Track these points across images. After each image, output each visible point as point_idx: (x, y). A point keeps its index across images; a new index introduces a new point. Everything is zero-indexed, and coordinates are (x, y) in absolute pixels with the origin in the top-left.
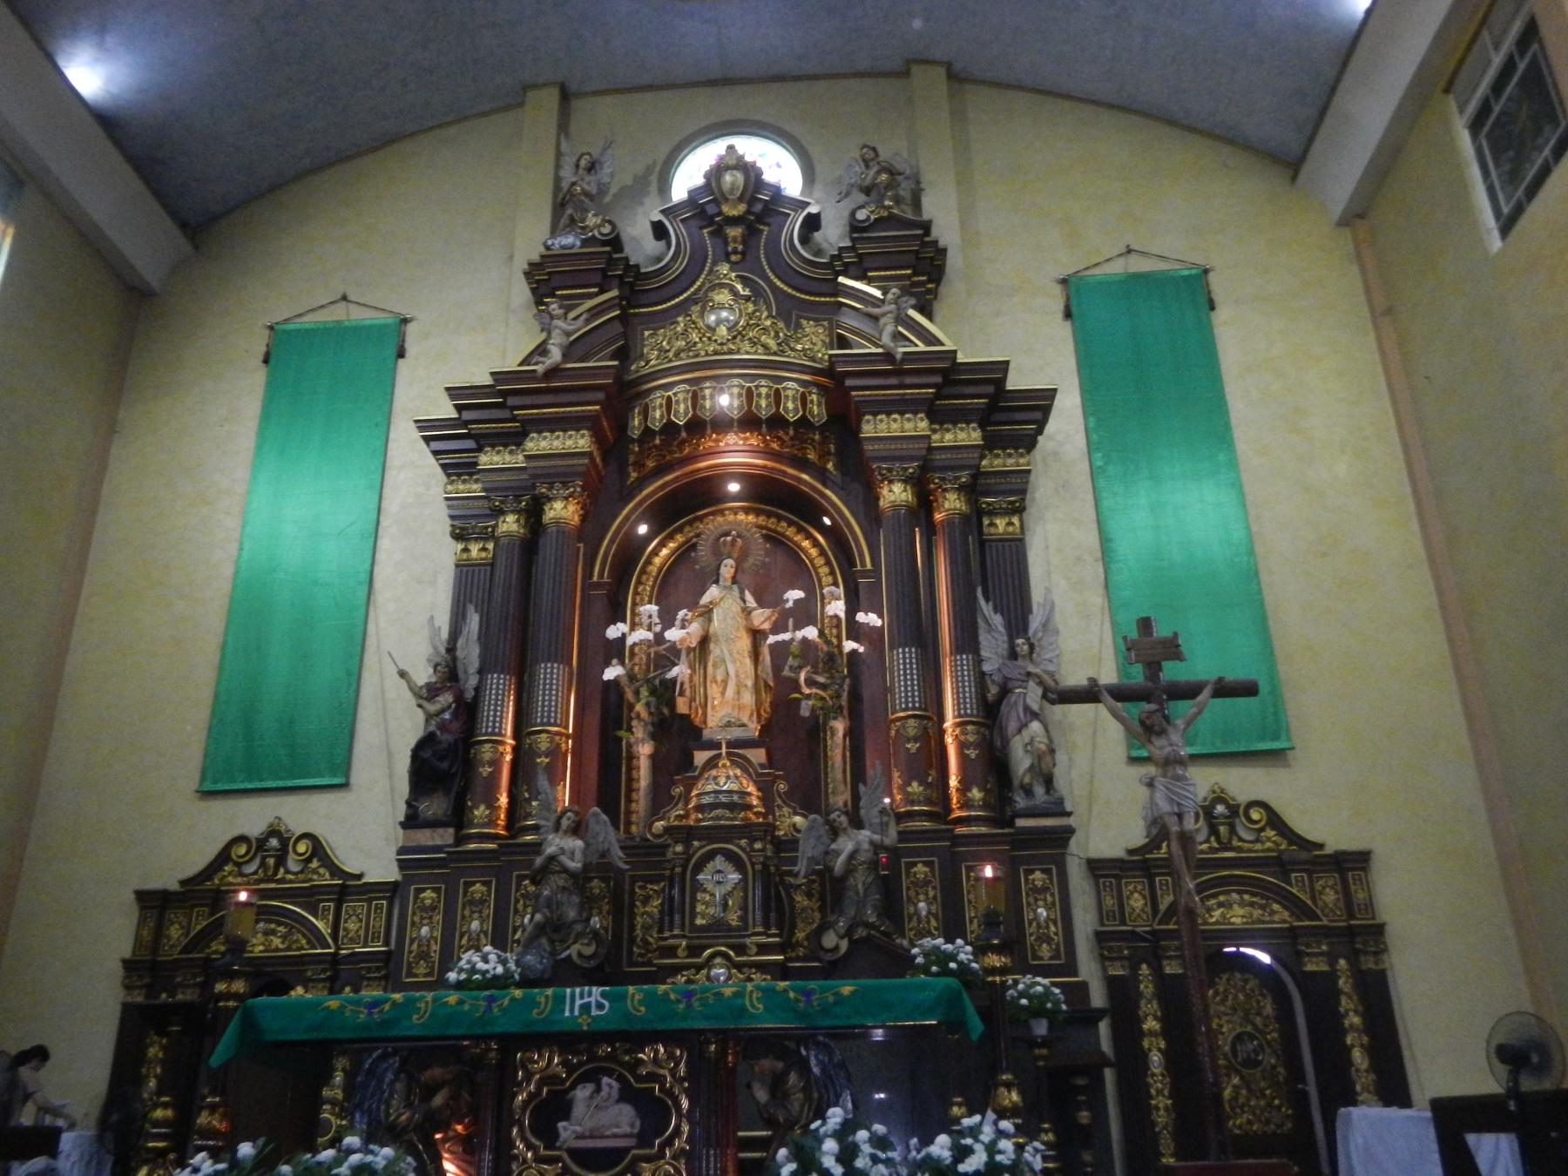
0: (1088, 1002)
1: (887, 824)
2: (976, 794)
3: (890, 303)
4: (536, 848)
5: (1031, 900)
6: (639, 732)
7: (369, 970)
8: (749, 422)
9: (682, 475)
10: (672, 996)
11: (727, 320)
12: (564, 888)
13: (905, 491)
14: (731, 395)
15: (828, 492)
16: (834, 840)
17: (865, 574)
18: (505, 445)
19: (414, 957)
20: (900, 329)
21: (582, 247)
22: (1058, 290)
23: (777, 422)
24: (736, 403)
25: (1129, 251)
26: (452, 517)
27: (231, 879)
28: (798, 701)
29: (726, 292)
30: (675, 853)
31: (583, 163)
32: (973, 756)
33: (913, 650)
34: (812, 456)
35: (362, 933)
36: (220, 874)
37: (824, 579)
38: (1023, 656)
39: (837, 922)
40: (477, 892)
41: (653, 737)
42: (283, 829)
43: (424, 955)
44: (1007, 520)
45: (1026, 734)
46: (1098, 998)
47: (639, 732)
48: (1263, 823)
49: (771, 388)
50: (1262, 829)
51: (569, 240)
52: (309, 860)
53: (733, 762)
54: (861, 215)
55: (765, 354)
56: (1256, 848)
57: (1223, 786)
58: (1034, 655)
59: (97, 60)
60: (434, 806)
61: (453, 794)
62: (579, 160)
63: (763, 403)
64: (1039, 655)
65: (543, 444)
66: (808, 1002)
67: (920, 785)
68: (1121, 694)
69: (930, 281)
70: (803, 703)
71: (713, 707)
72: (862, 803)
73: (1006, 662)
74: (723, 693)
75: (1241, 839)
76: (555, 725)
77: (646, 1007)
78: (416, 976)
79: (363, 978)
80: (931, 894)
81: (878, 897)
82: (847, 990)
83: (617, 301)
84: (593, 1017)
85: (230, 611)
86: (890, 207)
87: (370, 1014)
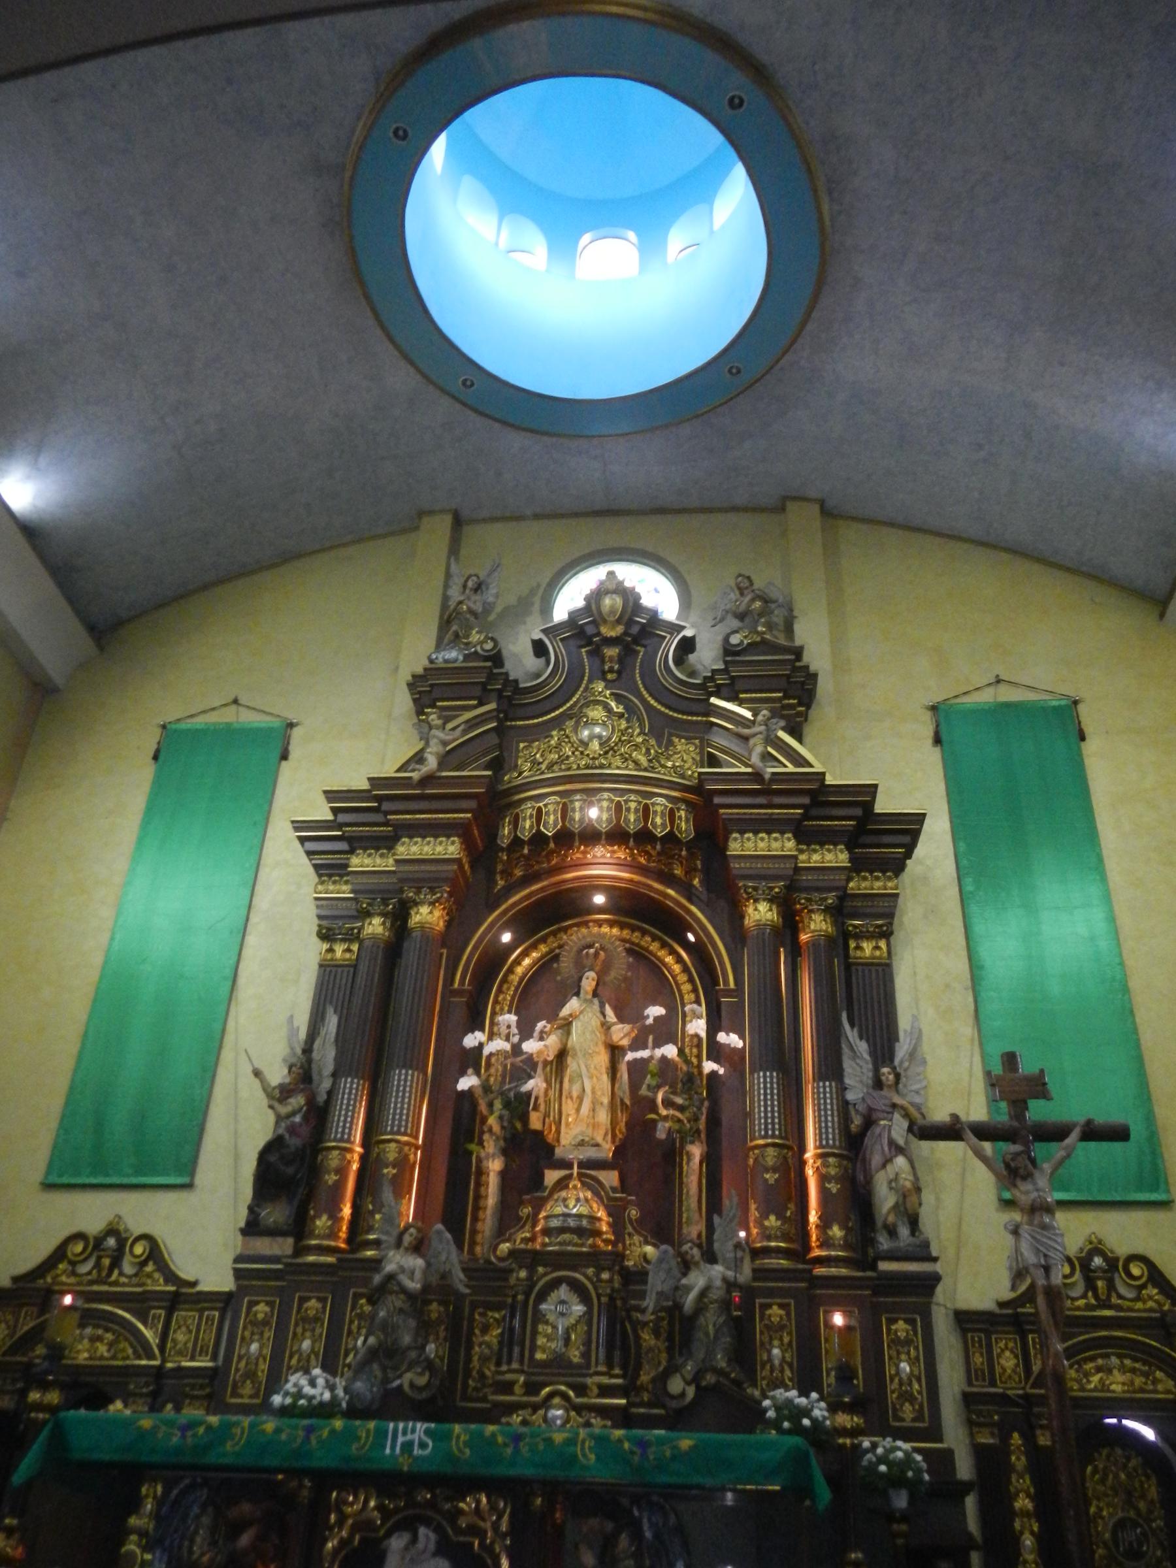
0: (955, 1474)
1: (742, 1260)
2: (836, 1232)
4: (376, 1264)
5: (894, 1353)
6: (490, 1146)
7: (193, 1387)
8: (617, 836)
9: (548, 886)
10: (500, 1440)
11: (600, 737)
12: (401, 1310)
13: (771, 910)
14: (601, 809)
15: (693, 909)
16: (685, 1274)
17: (729, 993)
18: (377, 849)
19: (241, 1376)
20: (770, 749)
21: (463, 661)
22: (927, 716)
23: (644, 837)
24: (605, 816)
25: (998, 681)
26: (320, 917)
27: (64, 1278)
28: (654, 1122)
29: (600, 708)
30: (518, 1279)
31: (470, 584)
32: (834, 1191)
33: (775, 1074)
34: (678, 872)
35: (190, 1345)
36: (53, 1273)
37: (686, 997)
38: (889, 1086)
39: (684, 1365)
40: (311, 1308)
41: (505, 1152)
42: (122, 1228)
43: (251, 1375)
44: (874, 944)
45: (889, 1167)
46: (964, 1469)
47: (490, 1146)
48: (1144, 1279)
49: (640, 803)
50: (1144, 1286)
51: (453, 654)
52: (144, 1263)
53: (584, 1184)
54: (735, 640)
55: (636, 770)
56: (1136, 1307)
57: (1101, 1236)
58: (901, 1086)
59: (28, 477)
60: (275, 1214)
62: (466, 581)
63: (632, 817)
64: (905, 1086)
65: (414, 849)
66: (644, 1454)
67: (777, 1219)
68: (983, 1132)
69: (800, 704)
70: (660, 1125)
71: (568, 1124)
72: (716, 1237)
73: (871, 1091)
74: (578, 1110)
75: (1120, 1297)
76: (405, 1134)
77: (471, 1449)
78: (241, 1396)
79: (187, 1396)
80: (786, 1339)
81: (728, 1339)
82: (686, 1443)
83: (495, 714)
84: (417, 1458)
85: (95, 1000)
86: (764, 633)
87: (183, 1436)
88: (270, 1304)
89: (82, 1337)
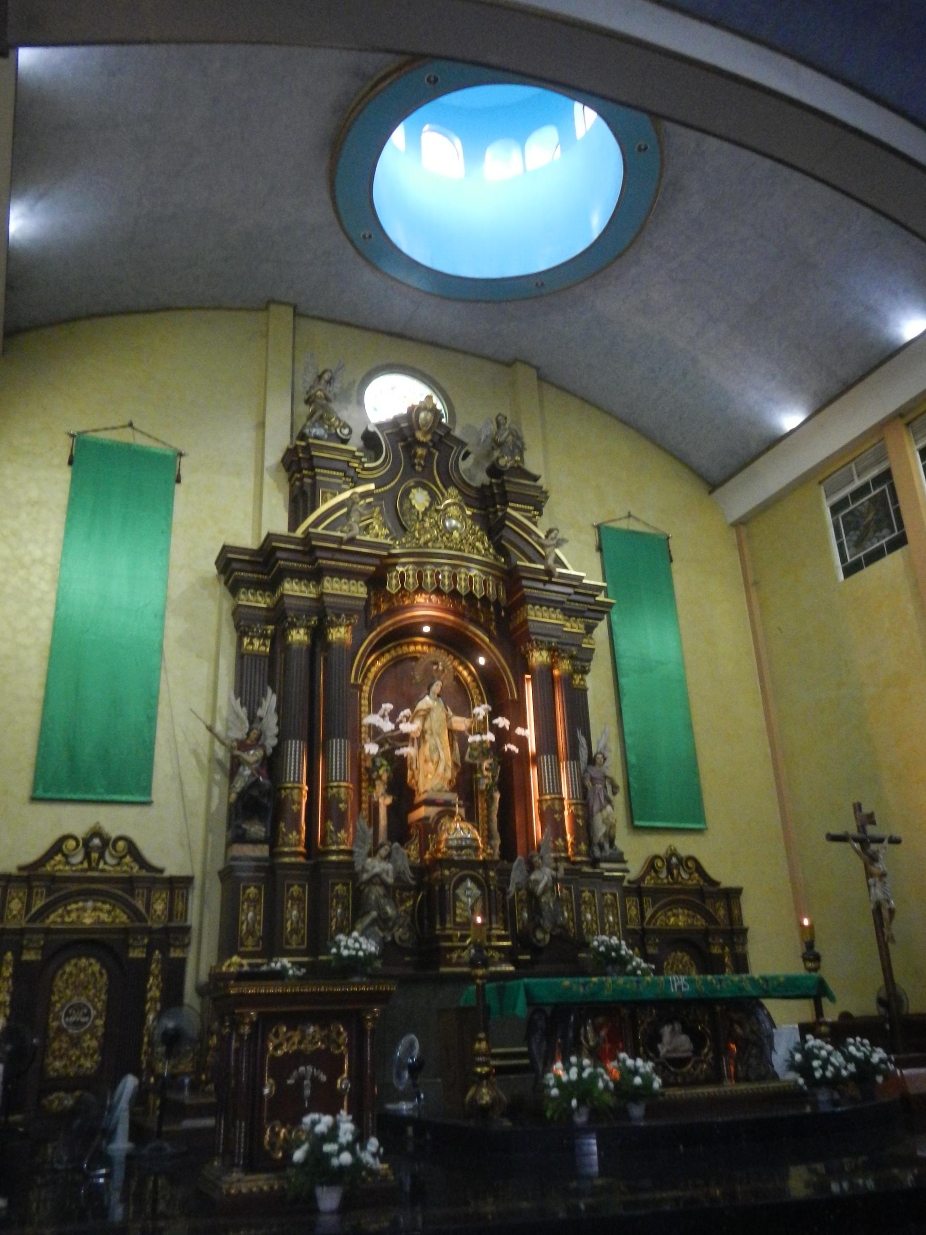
2: (583, 847)
3: (552, 539)
6: (380, 788)
10: (714, 981)
11: (456, 528)
17: (513, 701)
18: (300, 579)
25: (629, 516)
27: (61, 867)
35: (167, 913)
36: (52, 862)
41: (389, 791)
45: (604, 813)
51: (319, 431)
52: (124, 856)
60: (257, 829)
61: (269, 819)
62: (324, 372)
66: (768, 985)
70: (481, 781)
74: (436, 769)
75: (682, 878)
78: (246, 946)
88: (259, 888)
89: (84, 909)
